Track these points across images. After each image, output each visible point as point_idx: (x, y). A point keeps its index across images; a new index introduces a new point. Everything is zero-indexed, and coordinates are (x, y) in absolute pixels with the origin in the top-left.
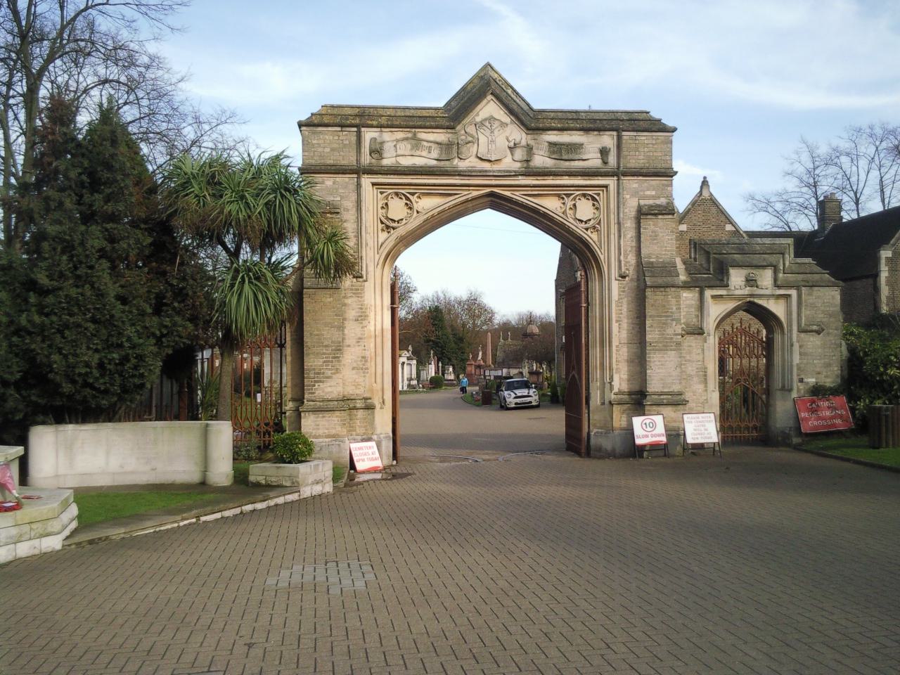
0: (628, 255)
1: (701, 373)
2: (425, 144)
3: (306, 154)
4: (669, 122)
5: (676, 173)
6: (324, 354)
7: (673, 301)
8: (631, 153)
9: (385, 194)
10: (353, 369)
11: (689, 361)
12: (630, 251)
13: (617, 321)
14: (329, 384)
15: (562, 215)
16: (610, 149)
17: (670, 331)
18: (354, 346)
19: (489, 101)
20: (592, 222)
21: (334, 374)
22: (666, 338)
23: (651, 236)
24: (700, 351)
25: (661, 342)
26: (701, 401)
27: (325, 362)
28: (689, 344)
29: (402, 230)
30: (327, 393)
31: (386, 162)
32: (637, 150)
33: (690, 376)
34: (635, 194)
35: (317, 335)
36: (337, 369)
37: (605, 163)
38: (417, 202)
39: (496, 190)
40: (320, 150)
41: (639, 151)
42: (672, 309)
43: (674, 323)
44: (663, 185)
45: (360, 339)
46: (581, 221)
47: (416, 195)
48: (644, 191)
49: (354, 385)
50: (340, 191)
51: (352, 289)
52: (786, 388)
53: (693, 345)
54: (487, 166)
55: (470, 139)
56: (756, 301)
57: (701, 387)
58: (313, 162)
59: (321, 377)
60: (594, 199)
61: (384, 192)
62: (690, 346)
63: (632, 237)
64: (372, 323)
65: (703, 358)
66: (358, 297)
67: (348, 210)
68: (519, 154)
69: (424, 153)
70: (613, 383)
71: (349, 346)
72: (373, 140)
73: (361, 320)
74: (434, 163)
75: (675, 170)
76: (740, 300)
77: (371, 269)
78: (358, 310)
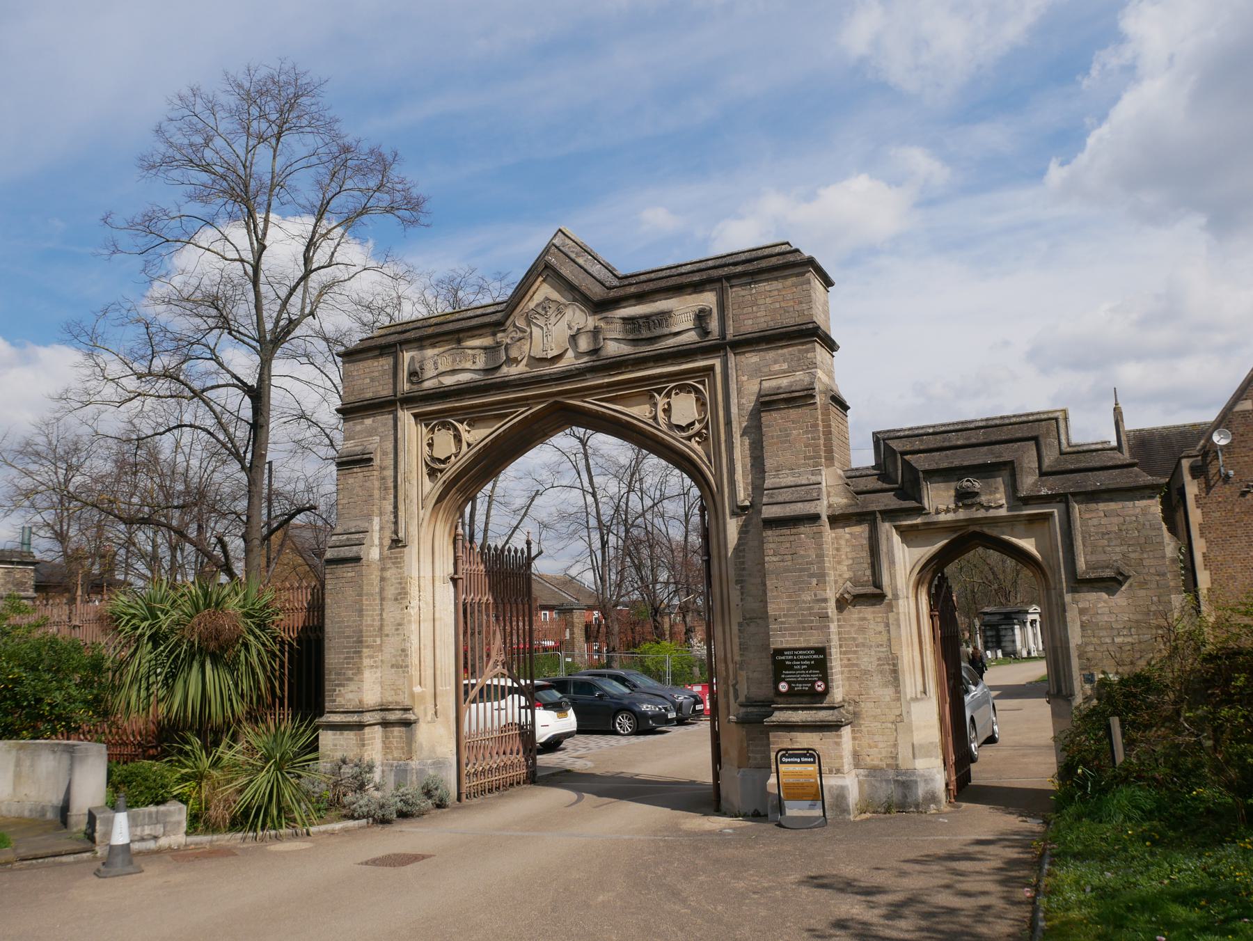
1: (887, 667)
2: (470, 352)
7: (810, 543)
10: (392, 666)
13: (737, 582)
14: (350, 689)
15: (651, 421)
20: (697, 426)
22: (801, 609)
23: (778, 437)
24: (881, 627)
25: (793, 616)
26: (892, 718)
27: (346, 658)
28: (861, 615)
29: (451, 470)
30: (350, 700)
31: (427, 385)
32: (754, 303)
33: (866, 672)
34: (756, 372)
37: (705, 332)
39: (559, 399)
40: (360, 382)
45: (400, 625)
51: (391, 558)
52: (1064, 692)
53: (870, 616)
56: (986, 530)
57: (888, 692)
58: (352, 399)
59: (345, 681)
62: (864, 619)
64: (414, 603)
65: (889, 640)
69: (468, 365)
76: (955, 531)
77: (413, 530)
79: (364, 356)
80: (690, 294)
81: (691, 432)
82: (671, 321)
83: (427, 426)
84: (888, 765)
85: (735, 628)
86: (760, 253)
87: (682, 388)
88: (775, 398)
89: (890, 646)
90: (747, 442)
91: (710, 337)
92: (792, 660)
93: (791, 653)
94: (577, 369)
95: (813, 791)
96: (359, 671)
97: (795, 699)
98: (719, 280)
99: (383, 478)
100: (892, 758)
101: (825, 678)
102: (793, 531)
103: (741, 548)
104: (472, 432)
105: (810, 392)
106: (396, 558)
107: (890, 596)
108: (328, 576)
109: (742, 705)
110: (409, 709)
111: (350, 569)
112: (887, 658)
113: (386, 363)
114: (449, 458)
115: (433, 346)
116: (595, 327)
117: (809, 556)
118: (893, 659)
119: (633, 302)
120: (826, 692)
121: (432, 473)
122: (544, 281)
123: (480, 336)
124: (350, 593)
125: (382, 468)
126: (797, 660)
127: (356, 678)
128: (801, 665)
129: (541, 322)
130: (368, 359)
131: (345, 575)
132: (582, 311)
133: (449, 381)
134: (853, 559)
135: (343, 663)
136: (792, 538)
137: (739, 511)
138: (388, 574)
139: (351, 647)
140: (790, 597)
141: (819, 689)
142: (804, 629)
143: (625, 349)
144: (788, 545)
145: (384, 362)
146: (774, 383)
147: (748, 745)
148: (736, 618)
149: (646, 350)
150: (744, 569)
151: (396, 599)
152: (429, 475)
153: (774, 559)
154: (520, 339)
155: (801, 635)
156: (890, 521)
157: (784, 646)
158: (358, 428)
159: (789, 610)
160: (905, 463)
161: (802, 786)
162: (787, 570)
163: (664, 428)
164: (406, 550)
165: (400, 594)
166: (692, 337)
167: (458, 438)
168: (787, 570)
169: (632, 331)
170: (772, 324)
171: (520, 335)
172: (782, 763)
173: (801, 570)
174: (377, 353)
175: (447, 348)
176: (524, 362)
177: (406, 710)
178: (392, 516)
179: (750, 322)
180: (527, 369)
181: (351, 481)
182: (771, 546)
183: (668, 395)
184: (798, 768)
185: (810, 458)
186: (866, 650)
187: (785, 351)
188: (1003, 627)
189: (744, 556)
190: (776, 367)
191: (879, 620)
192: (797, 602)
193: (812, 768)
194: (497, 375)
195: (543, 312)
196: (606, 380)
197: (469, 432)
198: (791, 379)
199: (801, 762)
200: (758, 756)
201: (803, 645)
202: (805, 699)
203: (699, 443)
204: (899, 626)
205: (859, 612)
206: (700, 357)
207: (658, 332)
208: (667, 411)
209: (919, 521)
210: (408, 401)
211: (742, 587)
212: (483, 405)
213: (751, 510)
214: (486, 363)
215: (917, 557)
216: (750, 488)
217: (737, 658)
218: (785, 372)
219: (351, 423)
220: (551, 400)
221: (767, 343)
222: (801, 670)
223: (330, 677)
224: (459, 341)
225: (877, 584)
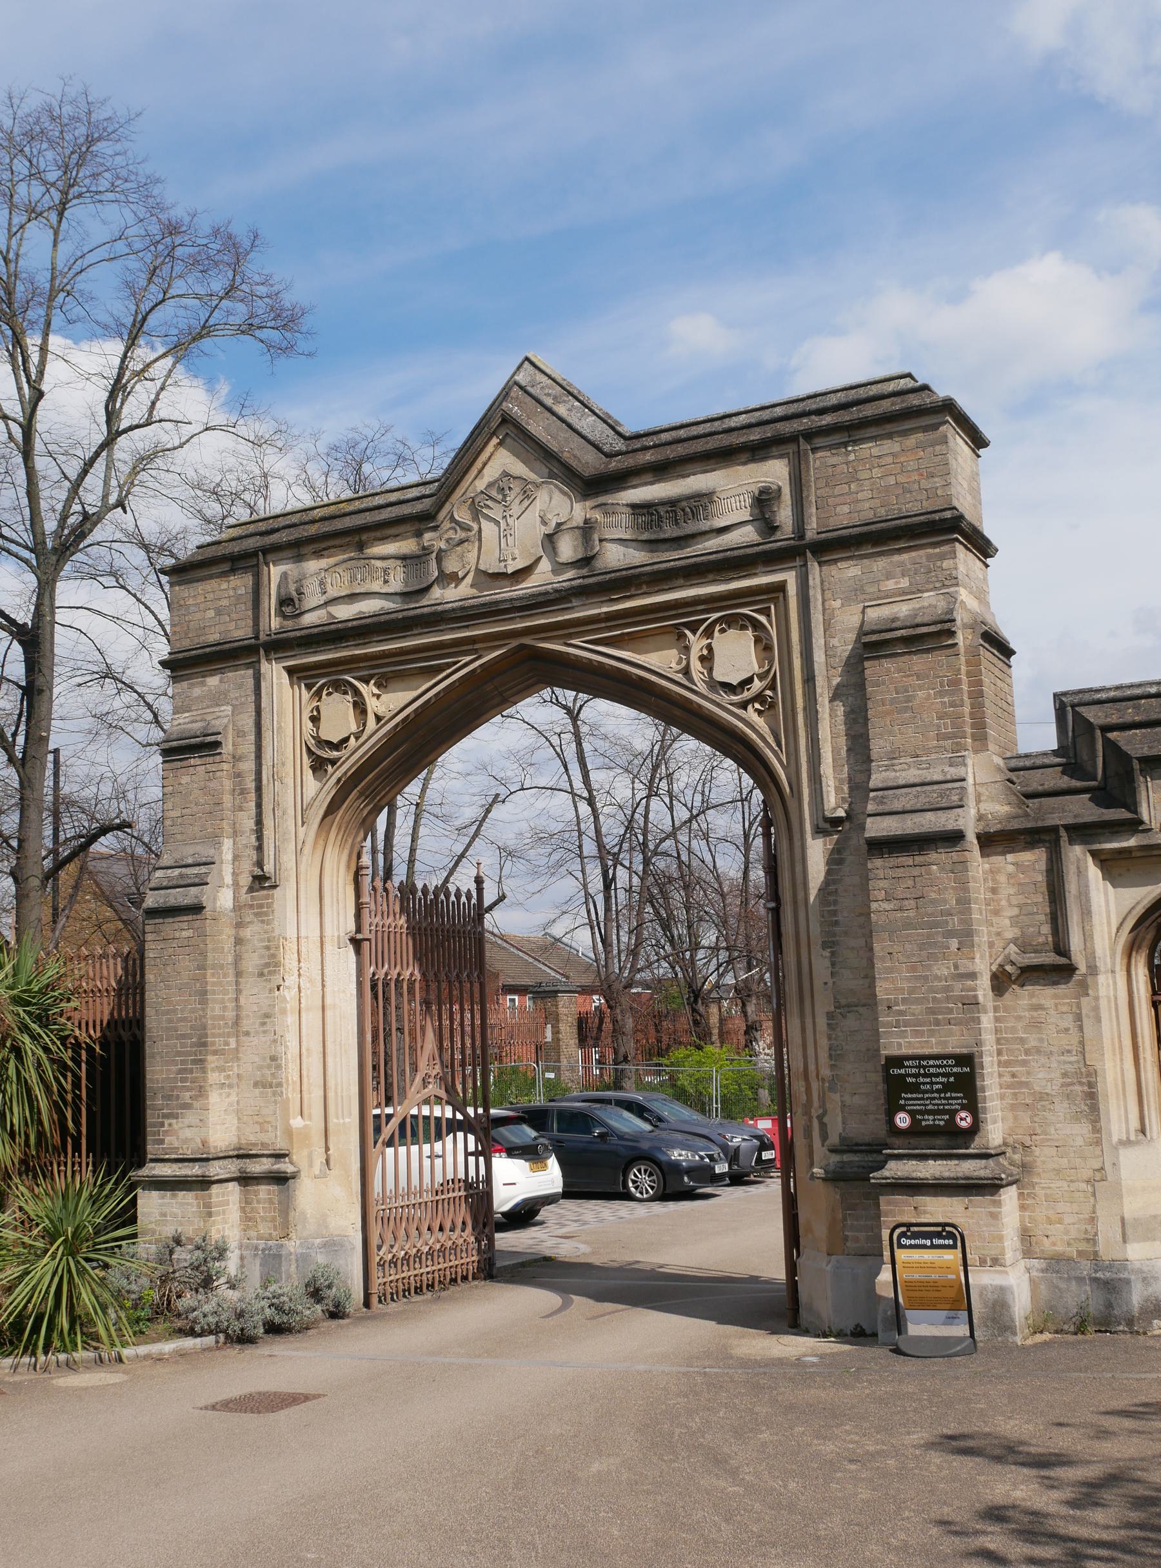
1: (1078, 1088)
6: (179, 1054)
7: (947, 880)
8: (837, 490)
10: (256, 1085)
13: (825, 946)
14: (186, 1122)
15: (679, 677)
16: (780, 489)
18: (257, 1032)
20: (757, 685)
22: (932, 990)
23: (893, 701)
24: (1068, 1022)
25: (918, 1001)
26: (1087, 1174)
27: (180, 1071)
28: (1035, 1001)
29: (350, 760)
30: (186, 1141)
31: (309, 619)
32: (853, 478)
33: (1042, 1096)
34: (856, 592)
36: (201, 1087)
37: (769, 527)
38: (378, 696)
39: (527, 641)
40: (198, 616)
45: (267, 1016)
46: (728, 687)
47: (372, 682)
50: (232, 696)
51: (251, 906)
53: (1048, 1003)
57: (1081, 1131)
58: (186, 644)
62: (1039, 1007)
64: (291, 980)
65: (1082, 1043)
66: (263, 922)
69: (377, 586)
70: (825, 1120)
71: (247, 1034)
73: (269, 972)
77: (288, 859)
78: (264, 952)
79: (205, 572)
80: (745, 464)
81: (746, 695)
82: (712, 508)
83: (309, 687)
84: (1080, 1253)
85: (822, 1022)
86: (862, 393)
87: (731, 622)
88: (888, 636)
89: (1083, 1053)
90: (840, 710)
91: (778, 535)
92: (916, 1076)
94: (556, 591)
95: (952, 1293)
96: (201, 1092)
97: (923, 1141)
98: (793, 438)
99: (238, 775)
100: (1088, 1240)
101: (973, 1107)
102: (919, 859)
103: (832, 888)
104: (384, 697)
105: (947, 626)
106: (261, 906)
107: (1082, 968)
108: (149, 937)
109: (833, 1151)
110: (284, 1156)
111: (185, 925)
112: (1078, 1073)
113: (240, 584)
114: (346, 740)
115: (318, 554)
116: (586, 521)
117: (945, 901)
118: (1089, 1075)
119: (649, 477)
120: (974, 1130)
121: (319, 766)
122: (500, 444)
123: (396, 537)
124: (186, 964)
125: (236, 759)
126: (925, 1075)
127: (196, 1104)
128: (932, 1083)
129: (496, 512)
130: (211, 577)
131: (177, 935)
132: (565, 494)
133: (344, 612)
134: (1020, 906)
136: (916, 871)
137: (827, 826)
138: (247, 933)
139: (189, 1054)
140: (913, 969)
141: (963, 1124)
142: (937, 1023)
143: (637, 557)
144: (910, 883)
145: (238, 582)
146: (885, 612)
147: (844, 1219)
148: (823, 1004)
149: (671, 557)
150: (836, 923)
151: (261, 975)
152: (314, 769)
153: (887, 906)
154: (462, 542)
155: (932, 1033)
156: (1084, 842)
157: (904, 1051)
158: (197, 692)
159: (912, 991)
160: (1107, 742)
161: (934, 1286)
162: (908, 925)
163: (702, 688)
164: (276, 892)
165: (267, 965)
166: (747, 535)
167: (360, 707)
168: (908, 925)
169: (648, 526)
170: (882, 512)
171: (461, 535)
172: (901, 1246)
173: (932, 925)
174: (226, 567)
175: (341, 557)
176: (469, 580)
177: (279, 1156)
178: (253, 838)
179: (846, 509)
180: (474, 592)
181: (185, 779)
182: (882, 884)
183: (709, 633)
184: (927, 1256)
185: (946, 737)
186: (1043, 1060)
187: (905, 557)
189: (835, 902)
190: (890, 585)
191: (1065, 1009)
192: (926, 978)
193: (951, 1257)
194: (424, 602)
195: (500, 497)
196: (605, 609)
197: (378, 696)
198: (915, 605)
199: (933, 1247)
200: (862, 1235)
201: (936, 1050)
202: (939, 1141)
203: (760, 712)
204: (1098, 1019)
205: (1032, 996)
206: (761, 569)
207: (690, 527)
208: (707, 659)
209: (1132, 842)
210: (277, 646)
211: (833, 954)
213: (847, 825)
214: (406, 583)
215: (1128, 903)
216: (846, 788)
217: (826, 1072)
218: (908, 594)
219: (185, 684)
220: (514, 643)
221: (875, 544)
222: (932, 1092)
223: (154, 1103)
224: (361, 547)
225: (1061, 948)
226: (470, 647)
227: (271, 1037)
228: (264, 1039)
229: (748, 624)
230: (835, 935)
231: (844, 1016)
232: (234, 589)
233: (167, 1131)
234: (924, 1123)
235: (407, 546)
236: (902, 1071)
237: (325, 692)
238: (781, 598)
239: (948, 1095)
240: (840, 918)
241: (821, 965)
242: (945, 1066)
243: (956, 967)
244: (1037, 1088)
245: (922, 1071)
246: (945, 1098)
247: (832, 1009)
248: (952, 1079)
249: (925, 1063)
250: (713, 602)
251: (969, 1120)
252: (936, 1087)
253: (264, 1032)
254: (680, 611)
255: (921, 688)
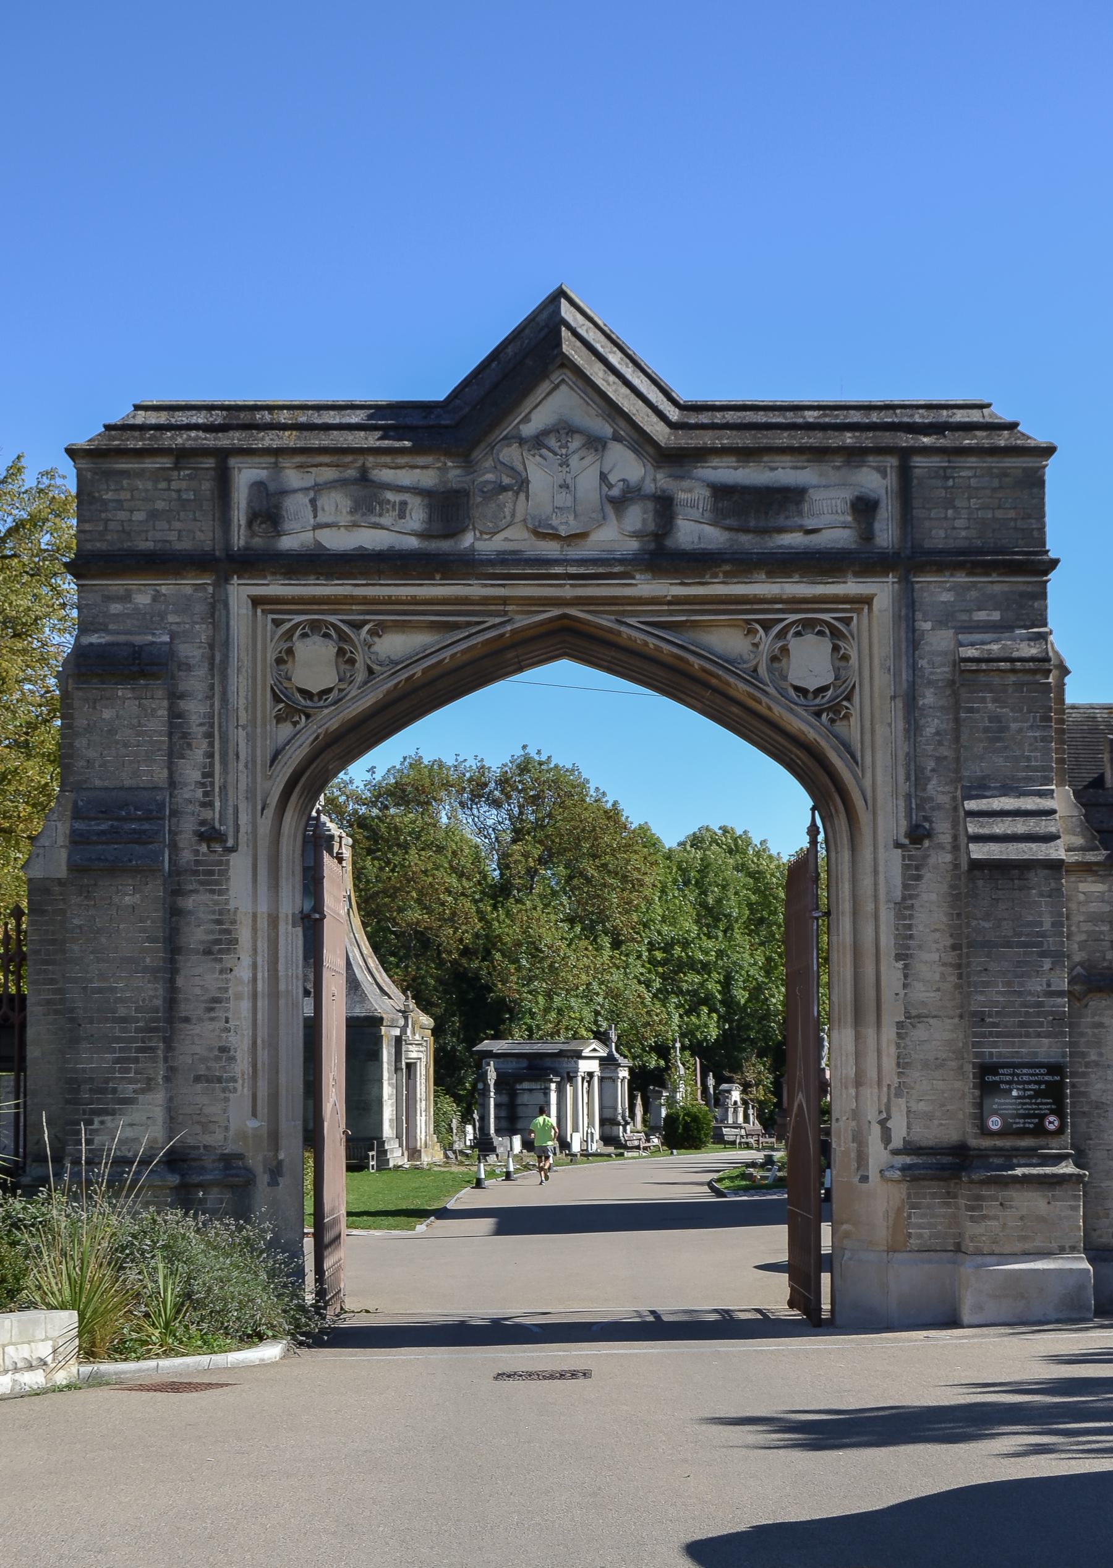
0: (929, 779)
2: (390, 496)
3: (87, 527)
4: (1036, 432)
5: (1055, 563)
6: (118, 1040)
9: (288, 626)
10: (198, 1079)
11: (1097, 1064)
12: (933, 770)
13: (898, 957)
17: (1036, 985)
18: (200, 1020)
19: (557, 387)
21: (143, 1091)
22: (1024, 1005)
23: (986, 730)
27: (118, 1061)
28: (1097, 1019)
31: (287, 543)
32: (949, 503)
35: (100, 990)
39: (573, 611)
40: (122, 515)
41: (954, 507)
42: (1041, 924)
43: (1047, 964)
44: (1022, 595)
47: (367, 628)
48: (970, 611)
49: (198, 1123)
51: (196, 873)
54: (550, 549)
55: (506, 480)
60: (835, 634)
61: (283, 621)
63: (937, 733)
66: (212, 892)
67: (189, 668)
68: (637, 517)
70: (889, 1124)
71: (187, 1020)
72: (258, 486)
73: (220, 951)
74: (413, 543)
75: (1052, 555)
85: (889, 1033)
93: (1010, 1071)
103: (909, 902)
106: (211, 873)
109: (896, 1152)
135: (112, 1070)
137: (907, 841)
138: (189, 903)
139: (133, 1040)
140: (1009, 984)
141: (1051, 1127)
142: (1028, 1035)
150: (911, 937)
151: (208, 952)
165: (218, 942)
181: (107, 714)
183: (782, 634)
188: (526, 1085)
189: (911, 917)
211: (906, 966)
212: (414, 601)
220: (556, 612)
226: (501, 608)
227: (222, 1024)
228: (211, 1027)
229: (827, 631)
230: (909, 948)
231: (914, 1026)
232: (179, 491)
233: (97, 1130)
234: (1015, 1126)
235: (427, 478)
236: (997, 1078)
237: (298, 633)
238: (866, 610)
239: (1039, 1101)
240: (914, 932)
241: (892, 974)
242: (1037, 1075)
243: (1049, 985)
244: (1093, 1098)
245: (1016, 1079)
246: (1035, 1104)
247: (902, 1019)
248: (1043, 1087)
249: (1018, 1071)
250: (795, 603)
251: (1056, 1123)
252: (1029, 1093)
253: (212, 1019)
254: (756, 607)
255: (1015, 720)
